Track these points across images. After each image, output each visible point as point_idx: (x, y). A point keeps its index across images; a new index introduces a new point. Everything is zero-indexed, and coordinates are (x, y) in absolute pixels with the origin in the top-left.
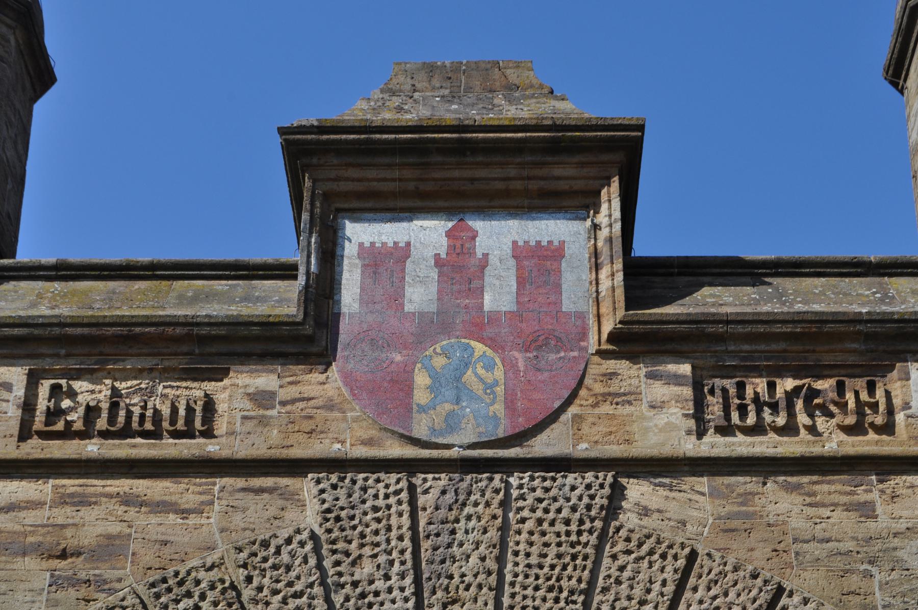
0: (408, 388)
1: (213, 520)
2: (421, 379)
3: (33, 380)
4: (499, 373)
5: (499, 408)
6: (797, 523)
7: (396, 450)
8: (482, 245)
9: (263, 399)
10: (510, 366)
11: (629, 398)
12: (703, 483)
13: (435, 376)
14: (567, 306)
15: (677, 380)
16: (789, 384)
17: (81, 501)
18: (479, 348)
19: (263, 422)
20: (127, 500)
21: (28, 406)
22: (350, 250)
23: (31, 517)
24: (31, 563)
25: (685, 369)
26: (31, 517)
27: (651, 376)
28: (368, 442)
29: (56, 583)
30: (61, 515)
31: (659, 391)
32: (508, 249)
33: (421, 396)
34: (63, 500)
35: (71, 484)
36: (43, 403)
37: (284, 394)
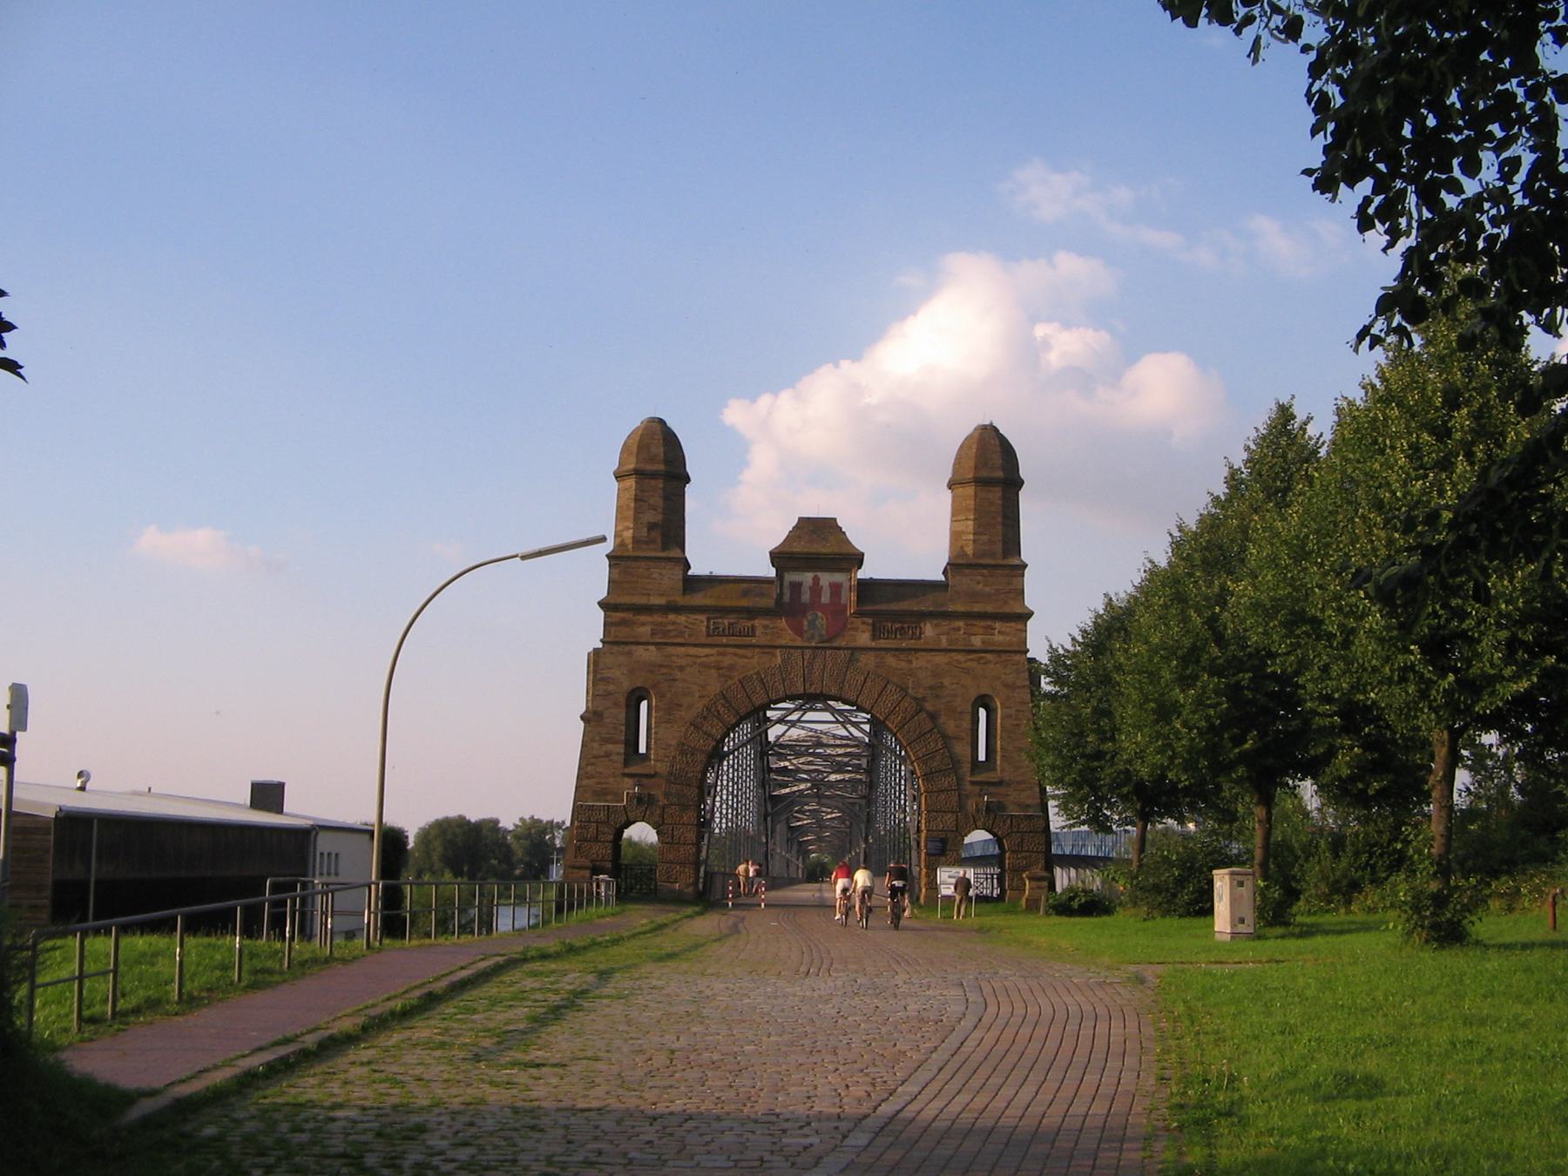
0: (802, 625)
1: (755, 660)
2: (806, 623)
3: (708, 620)
4: (825, 621)
5: (824, 632)
6: (894, 665)
7: (799, 643)
8: (821, 583)
9: (766, 627)
10: (827, 619)
11: (856, 629)
12: (872, 653)
13: (809, 622)
14: (843, 601)
15: (868, 624)
16: (897, 625)
17: (723, 654)
18: (820, 614)
19: (766, 634)
20: (735, 655)
21: (708, 627)
22: (786, 583)
23: (712, 659)
24: (713, 671)
25: (870, 621)
26: (712, 659)
27: (864, 623)
28: (793, 640)
29: (720, 676)
30: (720, 658)
31: (862, 627)
32: (827, 584)
33: (805, 628)
34: (719, 654)
35: (721, 650)
36: (712, 627)
37: (771, 626)
